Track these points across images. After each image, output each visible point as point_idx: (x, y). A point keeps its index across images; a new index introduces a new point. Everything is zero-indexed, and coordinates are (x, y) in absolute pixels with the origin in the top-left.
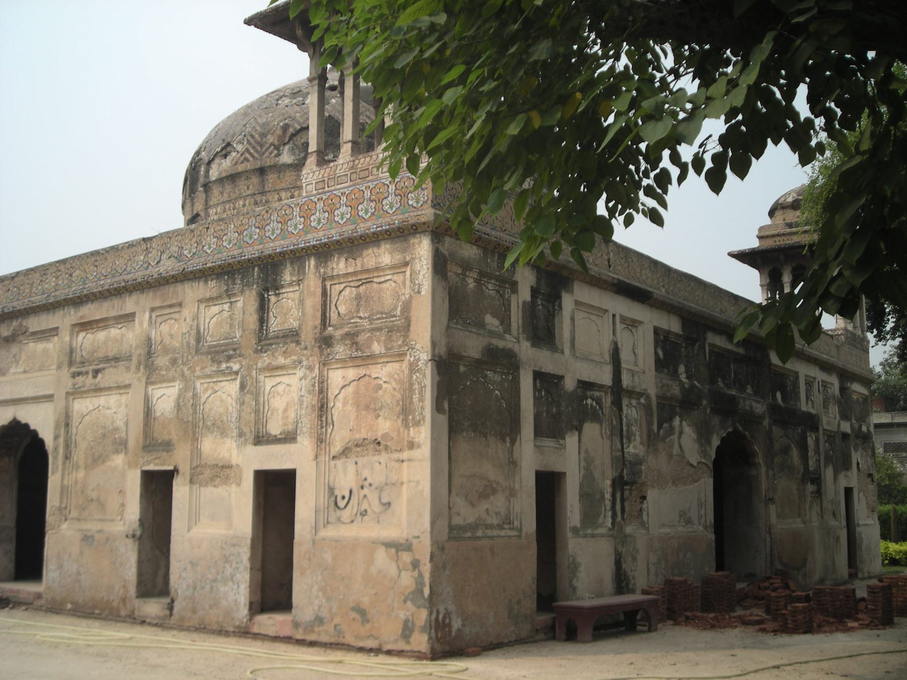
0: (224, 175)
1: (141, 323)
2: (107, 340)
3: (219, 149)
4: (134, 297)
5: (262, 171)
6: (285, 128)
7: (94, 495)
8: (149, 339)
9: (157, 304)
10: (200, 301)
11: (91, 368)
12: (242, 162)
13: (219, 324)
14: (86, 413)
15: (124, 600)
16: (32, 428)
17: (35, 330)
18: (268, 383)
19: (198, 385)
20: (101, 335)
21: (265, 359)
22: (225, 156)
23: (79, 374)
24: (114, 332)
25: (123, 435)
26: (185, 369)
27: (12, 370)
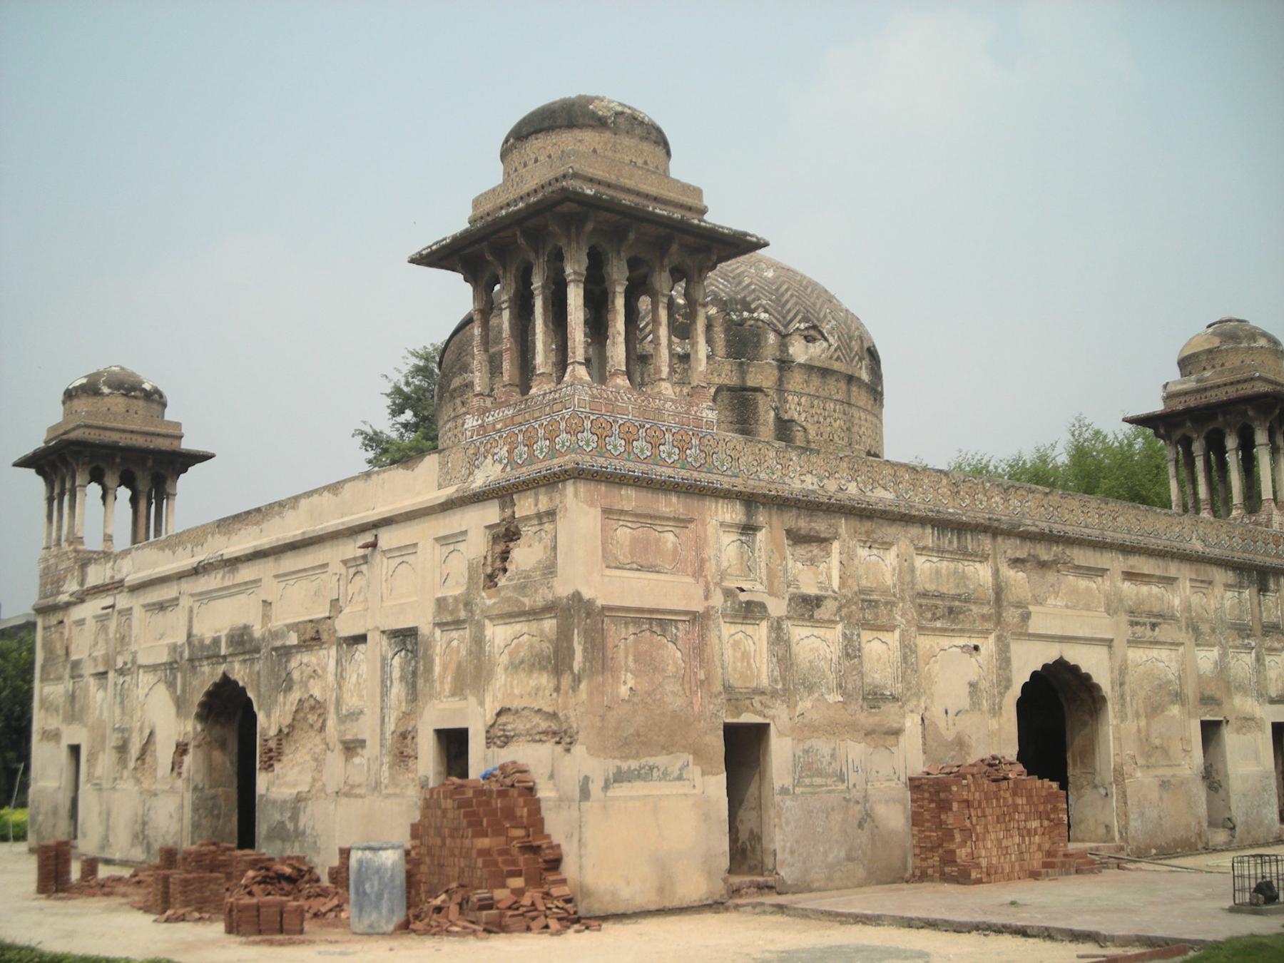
0: (817, 364)
1: (1184, 589)
2: (1150, 594)
3: (802, 326)
5: (850, 379)
7: (1157, 742)
9: (1194, 577)
13: (1232, 606)
14: (1140, 661)
15: (1200, 835)
16: (1084, 671)
17: (1082, 564)
18: (1268, 659)
20: (1144, 589)
21: (1268, 643)
23: (1137, 624)
24: (1155, 590)
25: (1177, 687)
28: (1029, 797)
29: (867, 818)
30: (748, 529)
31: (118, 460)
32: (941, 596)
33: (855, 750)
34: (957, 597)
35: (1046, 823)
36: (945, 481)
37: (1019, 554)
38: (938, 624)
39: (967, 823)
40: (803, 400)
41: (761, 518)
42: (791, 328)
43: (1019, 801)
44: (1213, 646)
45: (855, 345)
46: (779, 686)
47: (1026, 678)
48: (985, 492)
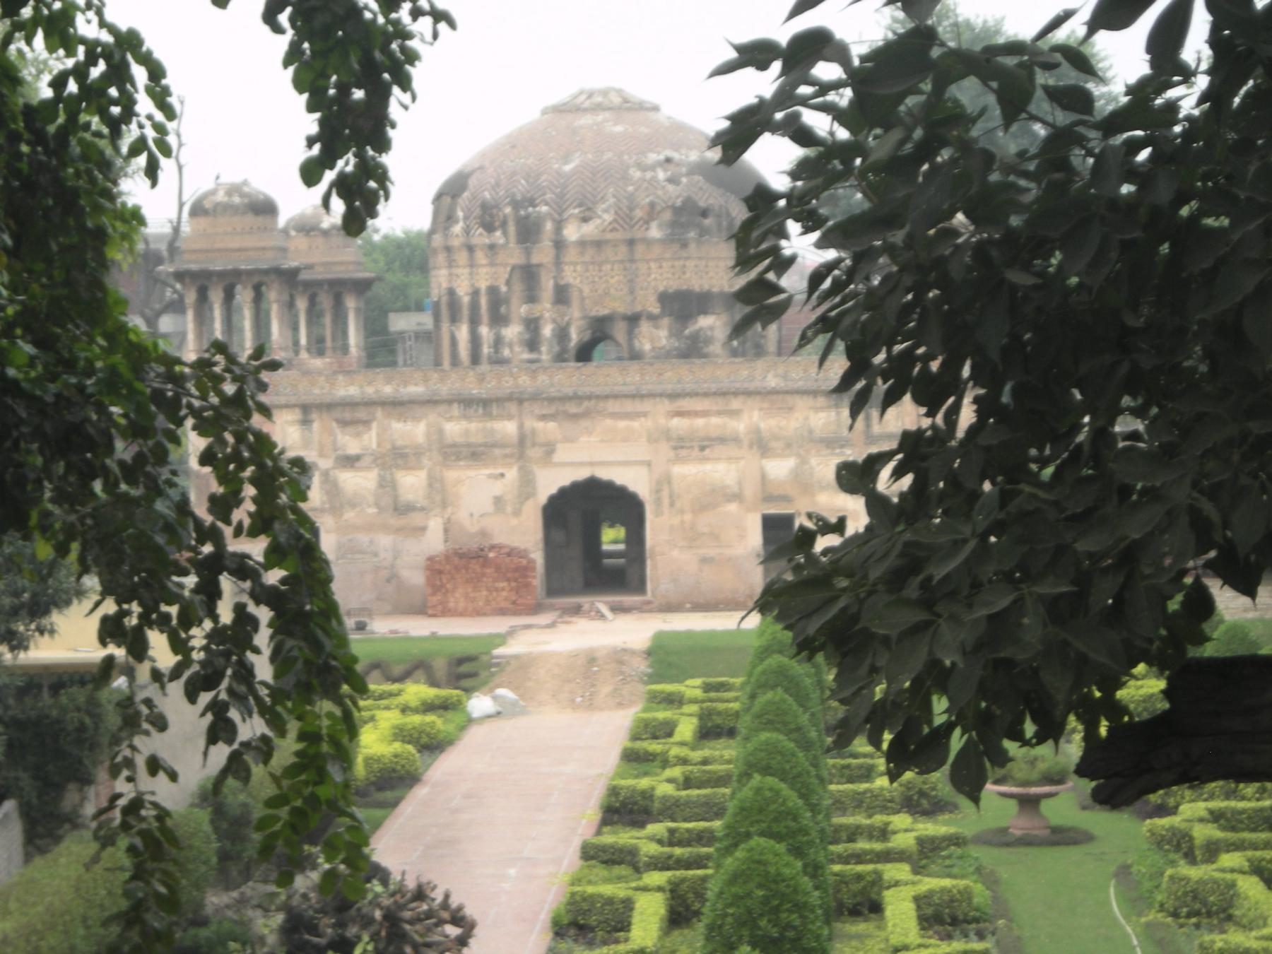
0: (589, 239)
4: (741, 399)
5: (631, 243)
6: (652, 205)
7: (706, 530)
8: (757, 431)
10: (811, 408)
11: (696, 444)
12: (611, 231)
19: (814, 461)
20: (700, 422)
22: (585, 220)
23: (682, 447)
24: (715, 420)
25: (736, 490)
26: (802, 452)
27: (583, 439)
28: (498, 568)
29: (393, 577)
30: (305, 422)
31: (301, 289)
32: (469, 445)
33: (385, 541)
34: (485, 445)
35: (513, 584)
36: (471, 373)
37: (545, 412)
38: (462, 463)
39: (438, 583)
40: (579, 268)
41: (314, 416)
42: (565, 216)
43: (488, 571)
44: (788, 456)
45: (638, 213)
46: (327, 506)
47: (553, 490)
48: (511, 375)
